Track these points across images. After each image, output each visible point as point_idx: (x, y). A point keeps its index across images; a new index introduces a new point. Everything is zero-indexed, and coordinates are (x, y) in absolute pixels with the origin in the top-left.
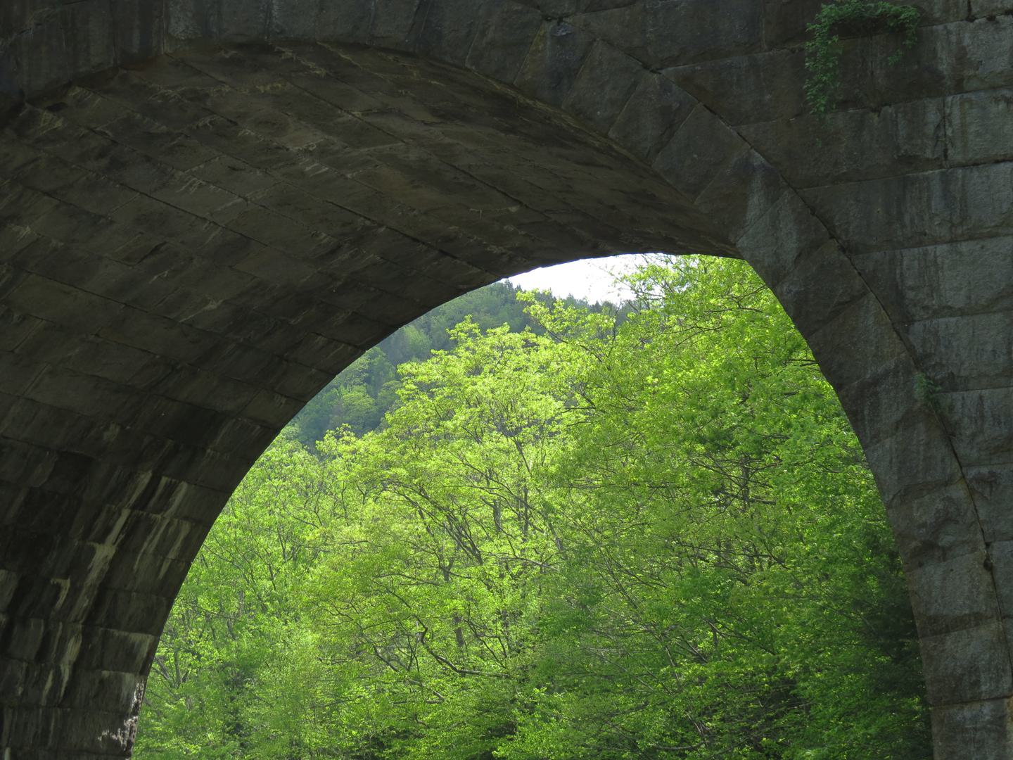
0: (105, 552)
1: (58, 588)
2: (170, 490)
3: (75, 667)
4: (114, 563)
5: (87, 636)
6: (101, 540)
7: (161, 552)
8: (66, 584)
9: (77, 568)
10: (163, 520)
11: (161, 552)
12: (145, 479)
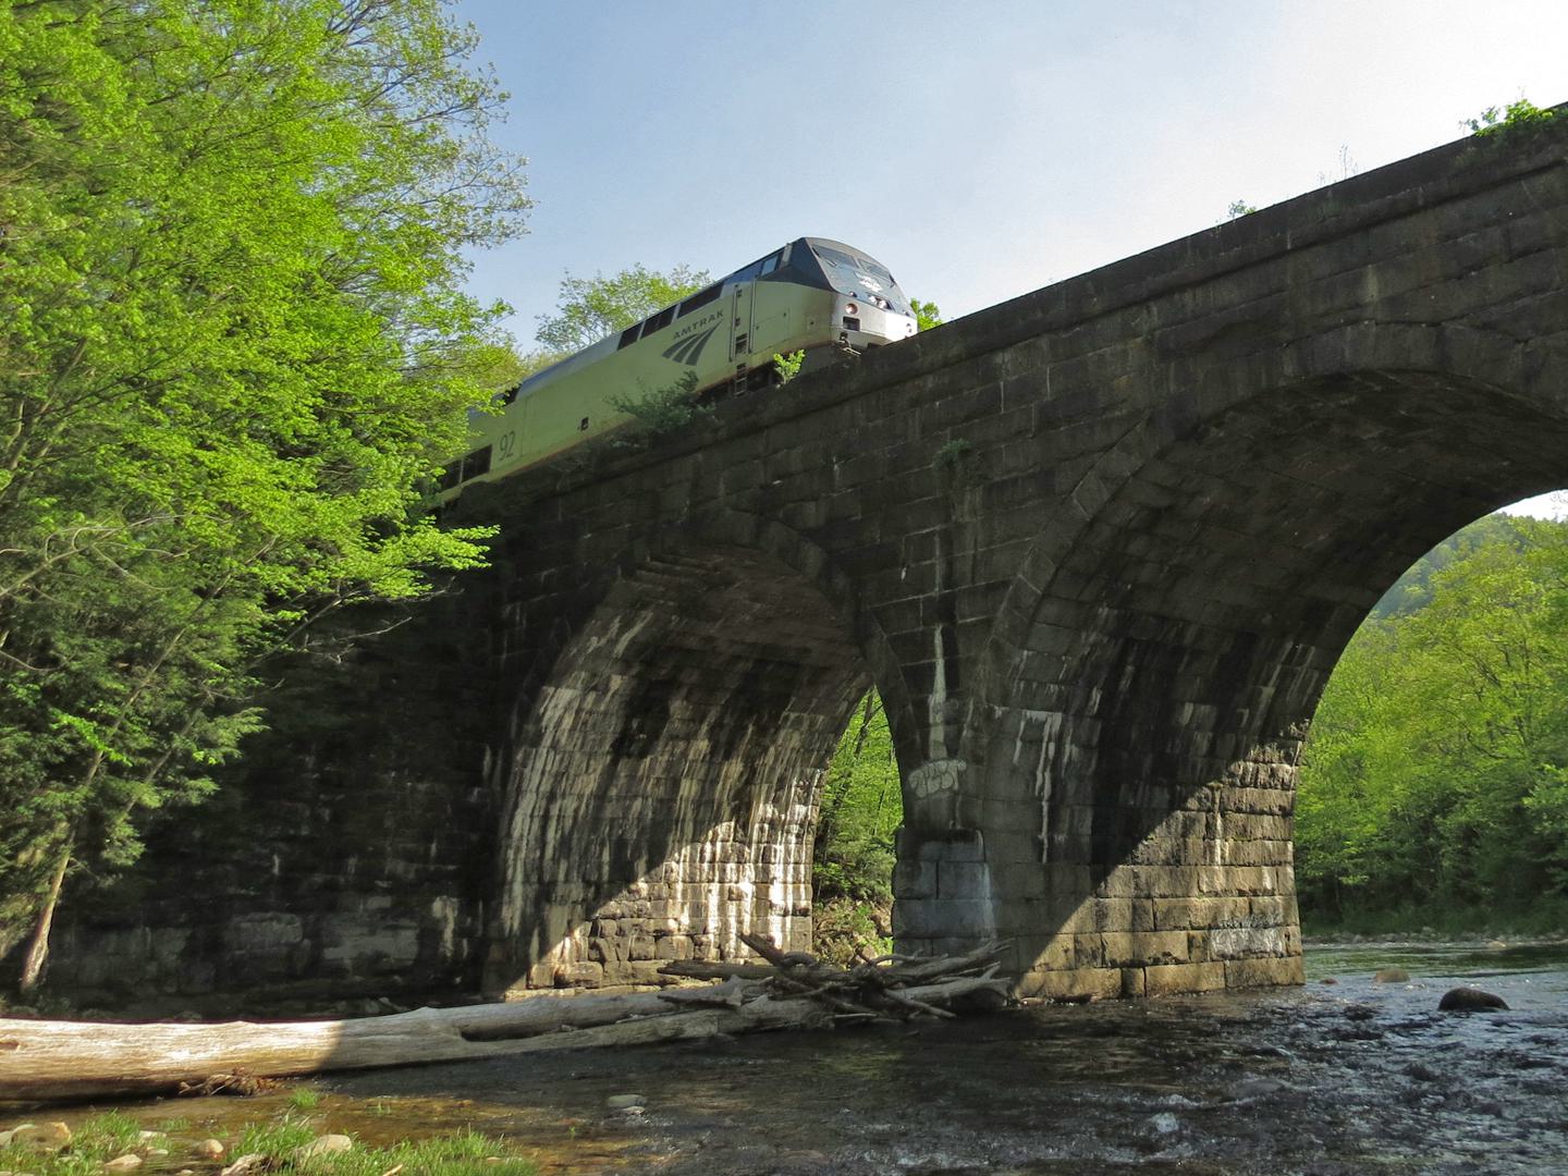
0: (1268, 691)
1: (1242, 714)
2: (1305, 652)
4: (1275, 698)
6: (1266, 684)
7: (1302, 690)
9: (1252, 702)
10: (1302, 670)
12: (1289, 646)
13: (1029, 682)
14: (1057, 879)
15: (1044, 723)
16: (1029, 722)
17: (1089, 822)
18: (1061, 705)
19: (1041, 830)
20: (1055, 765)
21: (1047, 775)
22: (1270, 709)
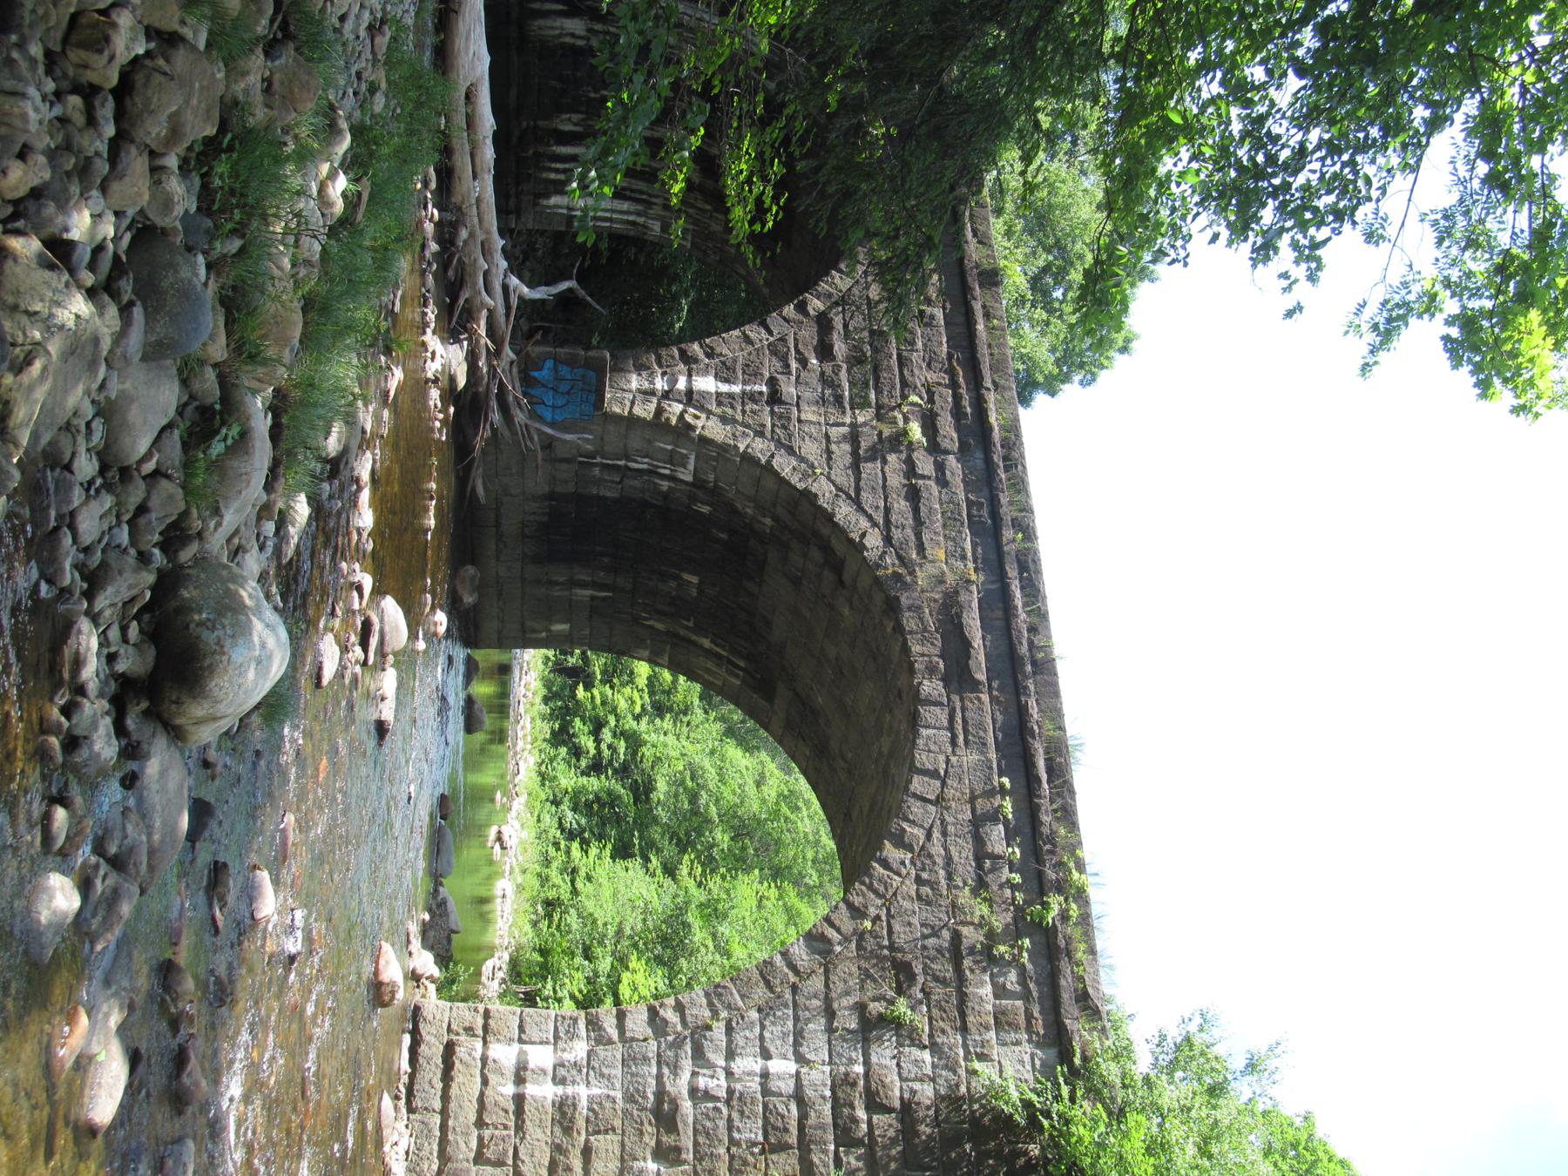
0: (706, 643)
2: (737, 676)
3: (652, 627)
4: (701, 647)
5: (668, 633)
6: (712, 641)
7: (708, 670)
8: (691, 624)
9: (699, 629)
11: (708, 670)
12: (742, 664)
13: (716, 459)
14: (564, 466)
16: (686, 457)
17: (609, 494)
18: (698, 483)
20: (652, 472)
22: (695, 644)
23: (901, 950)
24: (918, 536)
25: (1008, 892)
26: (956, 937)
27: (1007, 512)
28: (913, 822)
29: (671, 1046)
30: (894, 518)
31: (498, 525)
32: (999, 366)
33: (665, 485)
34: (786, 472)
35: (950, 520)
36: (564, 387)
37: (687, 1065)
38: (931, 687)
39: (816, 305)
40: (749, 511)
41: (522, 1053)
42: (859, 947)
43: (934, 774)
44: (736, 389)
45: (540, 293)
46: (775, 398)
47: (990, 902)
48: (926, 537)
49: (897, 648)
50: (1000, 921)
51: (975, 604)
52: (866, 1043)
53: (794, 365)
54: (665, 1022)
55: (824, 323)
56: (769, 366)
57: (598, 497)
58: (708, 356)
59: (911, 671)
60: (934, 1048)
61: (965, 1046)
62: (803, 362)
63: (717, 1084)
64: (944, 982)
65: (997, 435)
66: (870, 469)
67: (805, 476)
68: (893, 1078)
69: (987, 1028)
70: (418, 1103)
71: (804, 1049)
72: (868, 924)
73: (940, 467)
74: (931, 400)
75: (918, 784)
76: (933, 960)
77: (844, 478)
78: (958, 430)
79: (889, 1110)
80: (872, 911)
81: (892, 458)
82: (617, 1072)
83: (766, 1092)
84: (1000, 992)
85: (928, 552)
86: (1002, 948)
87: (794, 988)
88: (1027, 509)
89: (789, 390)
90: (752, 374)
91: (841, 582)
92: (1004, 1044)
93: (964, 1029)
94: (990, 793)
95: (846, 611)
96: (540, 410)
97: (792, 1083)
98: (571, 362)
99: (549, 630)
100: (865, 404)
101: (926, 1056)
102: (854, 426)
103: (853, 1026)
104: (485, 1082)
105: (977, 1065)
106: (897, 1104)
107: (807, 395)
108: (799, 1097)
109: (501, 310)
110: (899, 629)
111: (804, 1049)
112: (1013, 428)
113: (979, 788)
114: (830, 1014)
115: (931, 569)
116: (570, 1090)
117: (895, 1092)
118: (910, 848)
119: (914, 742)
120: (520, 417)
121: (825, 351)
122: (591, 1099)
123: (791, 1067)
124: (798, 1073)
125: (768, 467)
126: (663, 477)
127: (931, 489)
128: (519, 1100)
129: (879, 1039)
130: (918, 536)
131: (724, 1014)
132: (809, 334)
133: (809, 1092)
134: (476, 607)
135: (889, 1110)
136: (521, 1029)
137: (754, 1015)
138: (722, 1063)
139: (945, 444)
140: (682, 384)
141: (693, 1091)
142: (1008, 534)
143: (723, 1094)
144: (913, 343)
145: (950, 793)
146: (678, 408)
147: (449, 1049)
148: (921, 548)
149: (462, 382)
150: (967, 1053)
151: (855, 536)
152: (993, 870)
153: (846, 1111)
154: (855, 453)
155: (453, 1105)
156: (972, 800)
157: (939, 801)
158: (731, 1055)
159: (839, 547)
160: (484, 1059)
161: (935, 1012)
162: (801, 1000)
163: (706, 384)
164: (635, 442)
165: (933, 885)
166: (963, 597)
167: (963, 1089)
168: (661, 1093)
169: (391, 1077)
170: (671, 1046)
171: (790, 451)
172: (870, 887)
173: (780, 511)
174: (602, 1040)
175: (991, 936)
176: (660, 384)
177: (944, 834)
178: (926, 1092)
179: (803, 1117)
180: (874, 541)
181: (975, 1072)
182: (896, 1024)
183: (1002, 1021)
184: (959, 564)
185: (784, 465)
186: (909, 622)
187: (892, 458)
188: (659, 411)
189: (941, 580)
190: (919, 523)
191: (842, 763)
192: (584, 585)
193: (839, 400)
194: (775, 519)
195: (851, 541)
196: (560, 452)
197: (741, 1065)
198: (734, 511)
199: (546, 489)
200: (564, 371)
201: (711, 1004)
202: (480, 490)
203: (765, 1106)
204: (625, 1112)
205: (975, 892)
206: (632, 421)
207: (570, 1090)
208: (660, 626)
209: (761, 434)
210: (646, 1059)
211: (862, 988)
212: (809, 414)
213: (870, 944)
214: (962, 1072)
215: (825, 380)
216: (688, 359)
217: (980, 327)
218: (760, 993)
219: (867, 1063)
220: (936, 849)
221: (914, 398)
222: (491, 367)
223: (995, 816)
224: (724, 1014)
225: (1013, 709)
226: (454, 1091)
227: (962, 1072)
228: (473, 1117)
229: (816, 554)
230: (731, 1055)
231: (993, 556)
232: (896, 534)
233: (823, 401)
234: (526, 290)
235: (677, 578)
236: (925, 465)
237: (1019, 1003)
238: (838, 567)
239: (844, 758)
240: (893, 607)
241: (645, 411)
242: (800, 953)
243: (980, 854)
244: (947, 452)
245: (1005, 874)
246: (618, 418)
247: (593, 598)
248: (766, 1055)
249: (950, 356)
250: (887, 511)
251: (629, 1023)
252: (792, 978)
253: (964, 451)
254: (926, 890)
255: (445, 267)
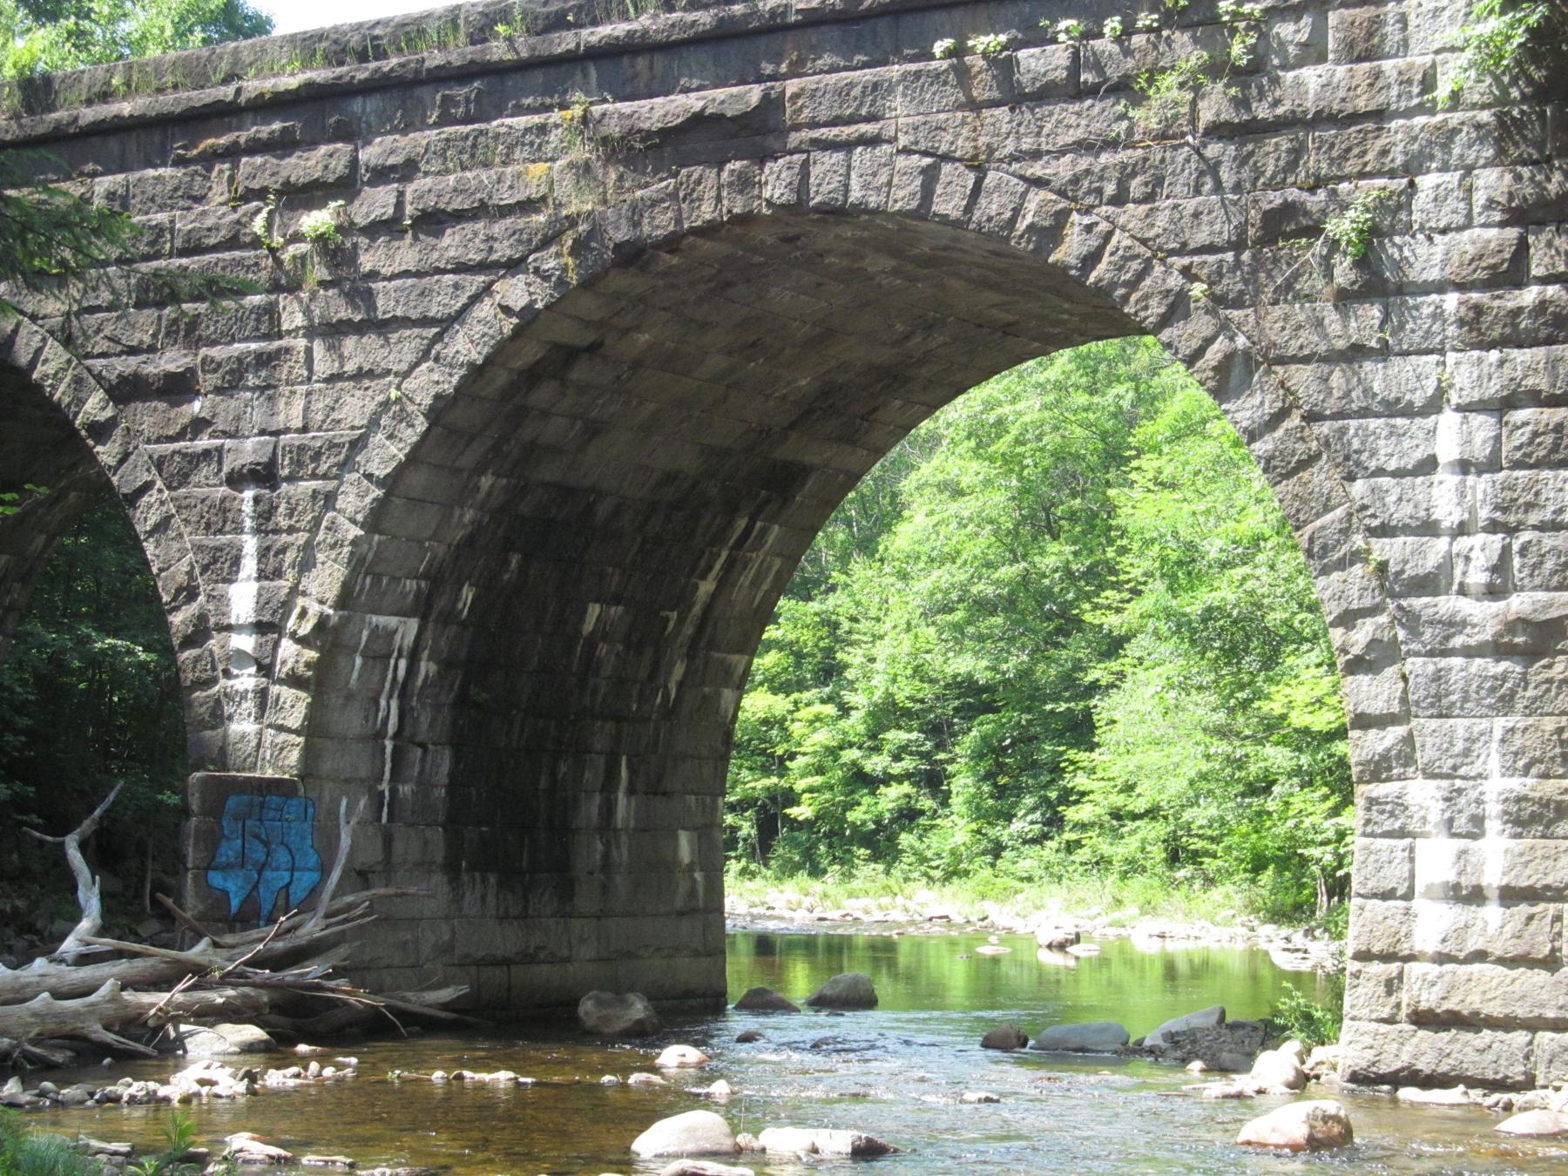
0: (706, 587)
1: (667, 619)
2: (764, 532)
3: (681, 685)
4: (714, 596)
5: (691, 657)
6: (703, 577)
7: (755, 583)
8: (674, 615)
9: (682, 600)
10: (757, 557)
11: (755, 583)
12: (742, 523)
14: (398, 847)
15: (396, 631)
16: (375, 632)
17: (445, 768)
18: (422, 608)
19: (380, 779)
20: (404, 691)
21: (394, 704)
22: (708, 608)
23: (1242, 229)
24: (505, 211)
25: (1138, 40)
26: (1218, 131)
27: (459, 52)
28: (1017, 212)
29: (1414, 632)
30: (474, 257)
31: (506, 962)
32: (196, 73)
33: (426, 667)
34: (397, 452)
35: (475, 154)
36: (258, 853)
37: (1447, 604)
38: (776, 183)
39: (95, 407)
40: (469, 515)
41: (1429, 894)
42: (1238, 303)
43: (930, 176)
44: (250, 544)
45: (90, 899)
46: (264, 475)
47: (1154, 73)
48: (508, 199)
49: (707, 245)
50: (1187, 52)
51: (626, 107)
52: (1404, 289)
53: (204, 442)
54: (1373, 643)
55: (127, 391)
56: (208, 487)
57: (452, 787)
58: (192, 595)
59: (746, 219)
60: (1412, 168)
61: (1409, 113)
62: (198, 426)
63: (1482, 549)
64: (1297, 152)
65: (321, 74)
66: (387, 302)
67: (403, 417)
68: (1468, 241)
69: (1377, 74)
70: (1516, 1072)
71: (1418, 399)
72: (1198, 289)
73: (381, 175)
74: (261, 194)
75: (948, 204)
76: (1258, 172)
77: (407, 345)
78: (313, 144)
79: (1522, 247)
80: (1175, 281)
81: (367, 262)
82: (1460, 725)
83: (1492, 464)
84: (1313, 52)
85: (534, 192)
86: (1237, 49)
87: (1312, 417)
88: (452, 18)
89: (249, 450)
90: (221, 517)
91: (593, 349)
92: (1405, 44)
93: (1380, 115)
94: (963, 74)
95: (644, 338)
96: (298, 892)
97: (1477, 419)
98: (211, 840)
99: (690, 868)
100: (271, 311)
101: (1426, 182)
102: (311, 332)
103: (1375, 312)
104: (1480, 956)
105: (1442, 92)
106: (1512, 233)
107: (257, 416)
108: (1502, 405)
109: (123, 967)
110: (672, 243)
111: (1418, 399)
112: (307, 45)
113: (954, 94)
114: (1356, 353)
115: (565, 188)
116: (1493, 808)
117: (1495, 238)
118: (1062, 217)
119: (875, 212)
120: (312, 928)
121: (178, 387)
122: (1509, 771)
123: (1449, 420)
124: (1459, 408)
125: (390, 483)
126: (412, 670)
127: (422, 190)
128: (1510, 896)
129: (1398, 266)
130: (505, 211)
131: (1358, 541)
132: (148, 416)
133: (1493, 388)
134: (654, 996)
135: (1522, 247)
136: (1388, 895)
137: (1359, 488)
138: (1442, 543)
139: (339, 166)
140: (245, 642)
141: (1493, 592)
142: (497, 51)
143: (1497, 540)
144: (159, 230)
145: (963, 147)
146: (287, 648)
147: (1424, 1019)
148: (528, 206)
149: (253, 1033)
150: (1421, 109)
151: (509, 324)
152: (1098, 67)
153: (1524, 323)
154: (360, 329)
155: (1521, 1012)
156: (975, 106)
157: (978, 166)
158: (1429, 528)
159: (530, 353)
160: (1442, 958)
161: (1351, 167)
162: (1331, 406)
163: (242, 599)
164: (352, 722)
165: (1126, 174)
166: (614, 129)
167: (1485, 116)
168: (1498, 649)
169: (1476, 1118)
170: (1414, 632)
171: (358, 444)
172: (1133, 285)
173: (468, 459)
174: (1406, 753)
175: (1214, 69)
176: (246, 680)
177: (1036, 155)
178: (1492, 182)
179: (1536, 399)
180: (516, 291)
181: (1455, 96)
182: (1372, 236)
183: (1364, 49)
184: (554, 137)
185: (385, 455)
186: (660, 224)
187: (367, 262)
188: (294, 680)
189: (587, 167)
190: (483, 211)
191: (917, 339)
192: (609, 808)
193: (264, 361)
194: (480, 469)
195: (518, 332)
196: (372, 854)
197: (1447, 512)
198: (470, 541)
199: (439, 879)
200: (228, 851)
201: (1342, 565)
202: (446, 994)
203: (1517, 465)
204: (1530, 711)
205: (1139, 99)
206: (313, 729)
207: (1493, 808)
208: (679, 671)
209: (330, 499)
210: (1438, 677)
211: (1309, 298)
212: (291, 413)
213: (1232, 284)
214: (1455, 118)
215: (232, 384)
216: (199, 633)
217: (126, 108)
218: (1321, 478)
219: (1441, 287)
220: (1063, 169)
221: (258, 225)
222: (226, 980)
223: (1003, 66)
224: (1358, 541)
225: (813, 36)
226: (1495, 1009)
227: (1455, 118)
228: (1541, 976)
229: (543, 395)
230: (1429, 528)
231: (539, 77)
232: (503, 251)
233: (267, 389)
234: (85, 925)
235: (591, 642)
236: (377, 202)
237: (1333, 18)
238: (567, 355)
239: (907, 337)
240: (633, 255)
241: (294, 706)
242: (1251, 407)
243: (1070, 89)
244: (354, 163)
245: (1104, 45)
246: (309, 753)
247: (631, 791)
248: (1429, 465)
249: (181, 162)
250: (461, 268)
251: (1377, 707)
252: (1294, 421)
253: (350, 133)
254: (1136, 187)
255: (46, 1068)
